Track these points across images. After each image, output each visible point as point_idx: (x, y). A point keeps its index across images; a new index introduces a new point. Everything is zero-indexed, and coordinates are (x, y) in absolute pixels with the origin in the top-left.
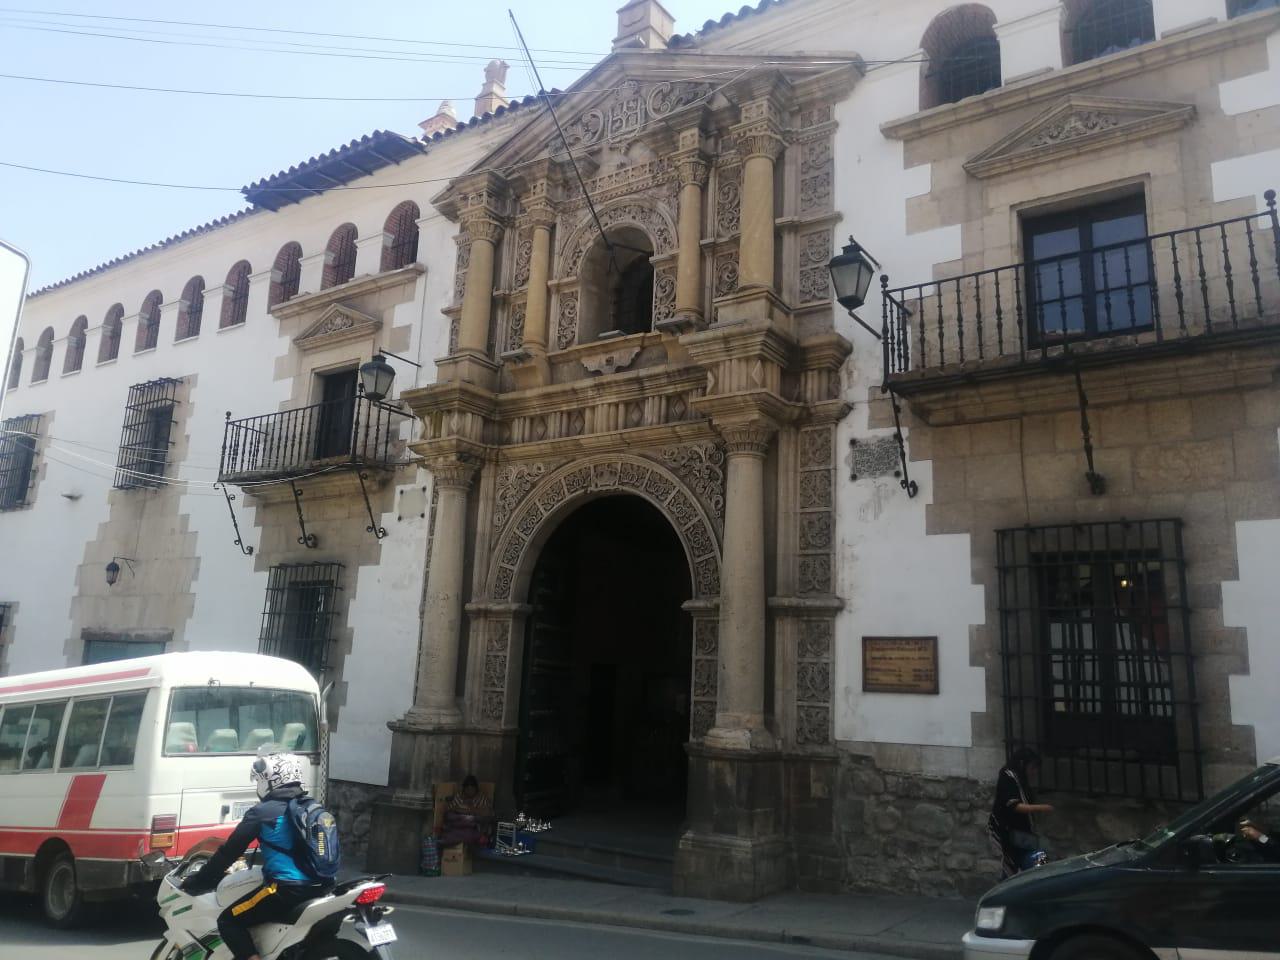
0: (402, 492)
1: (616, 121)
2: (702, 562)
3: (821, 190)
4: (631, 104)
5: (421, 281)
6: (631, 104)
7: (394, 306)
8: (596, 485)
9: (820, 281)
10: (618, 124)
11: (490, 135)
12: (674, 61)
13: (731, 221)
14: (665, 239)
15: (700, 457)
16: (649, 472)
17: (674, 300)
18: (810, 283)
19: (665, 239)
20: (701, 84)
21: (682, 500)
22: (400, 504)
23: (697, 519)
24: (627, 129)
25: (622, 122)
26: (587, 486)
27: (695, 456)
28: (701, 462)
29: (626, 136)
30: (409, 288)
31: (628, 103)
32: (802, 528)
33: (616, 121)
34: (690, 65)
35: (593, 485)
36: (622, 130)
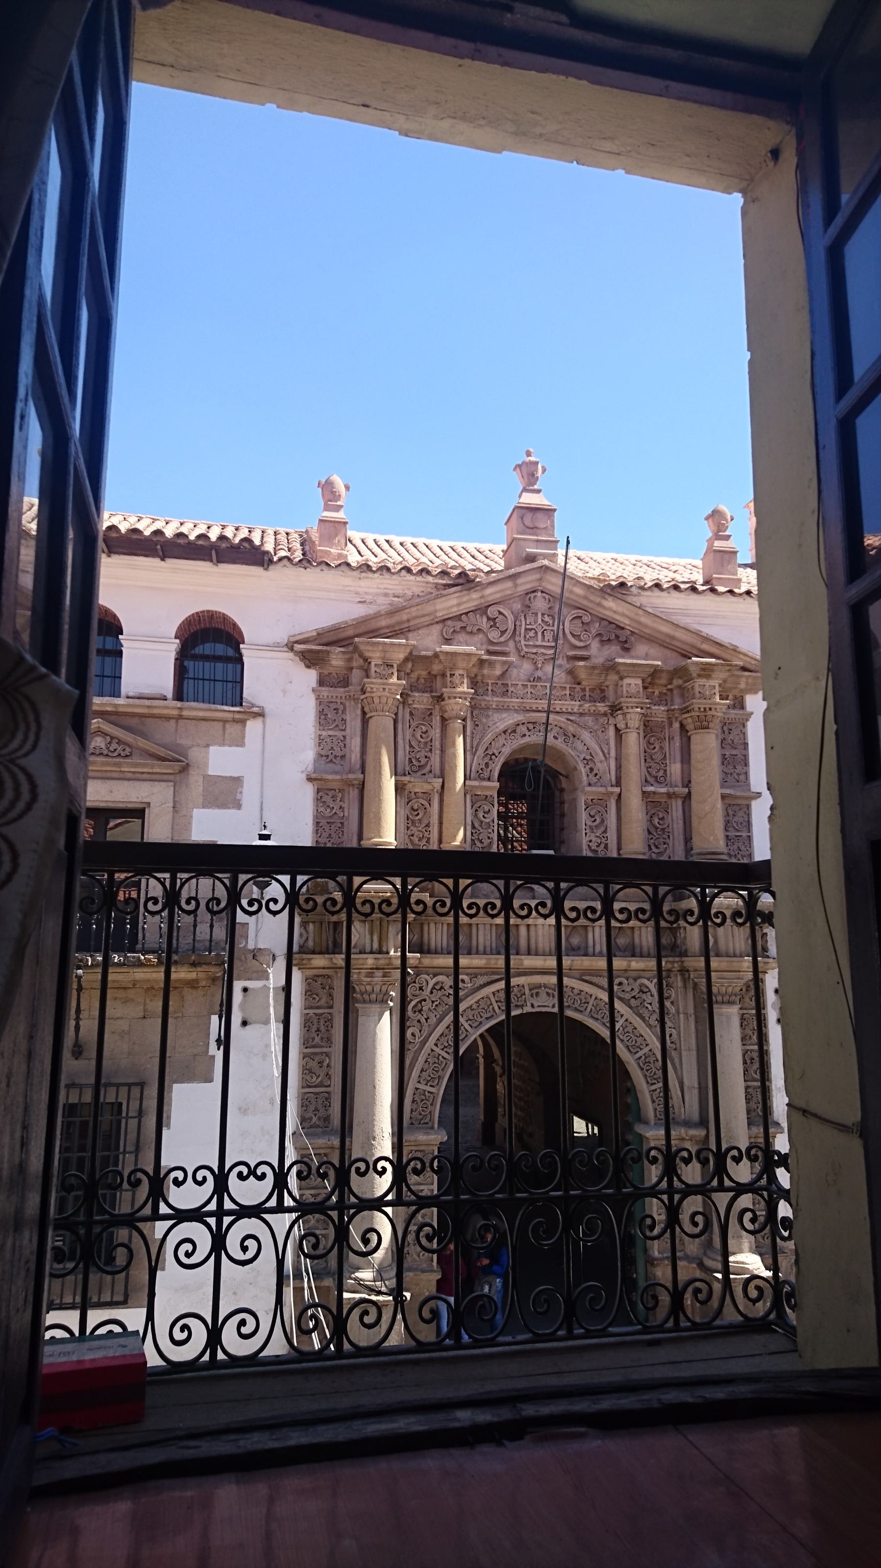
0: (245, 990)
1: (531, 630)
2: (656, 1090)
3: (739, 768)
4: (547, 619)
5: (253, 727)
6: (547, 619)
7: (208, 746)
8: (532, 1006)
9: (743, 848)
10: (532, 634)
11: (363, 583)
12: (604, 598)
13: (659, 770)
14: (591, 770)
15: (650, 991)
16: (593, 997)
17: (605, 832)
18: (735, 847)
19: (591, 770)
20: (623, 628)
21: (630, 1029)
22: (242, 1007)
23: (648, 1048)
24: (545, 644)
25: (536, 633)
26: (522, 1006)
27: (645, 990)
28: (652, 995)
29: (543, 651)
30: (232, 729)
31: (543, 615)
32: (745, 1062)
33: (531, 630)
34: (620, 609)
35: (529, 1004)
36: (539, 643)
